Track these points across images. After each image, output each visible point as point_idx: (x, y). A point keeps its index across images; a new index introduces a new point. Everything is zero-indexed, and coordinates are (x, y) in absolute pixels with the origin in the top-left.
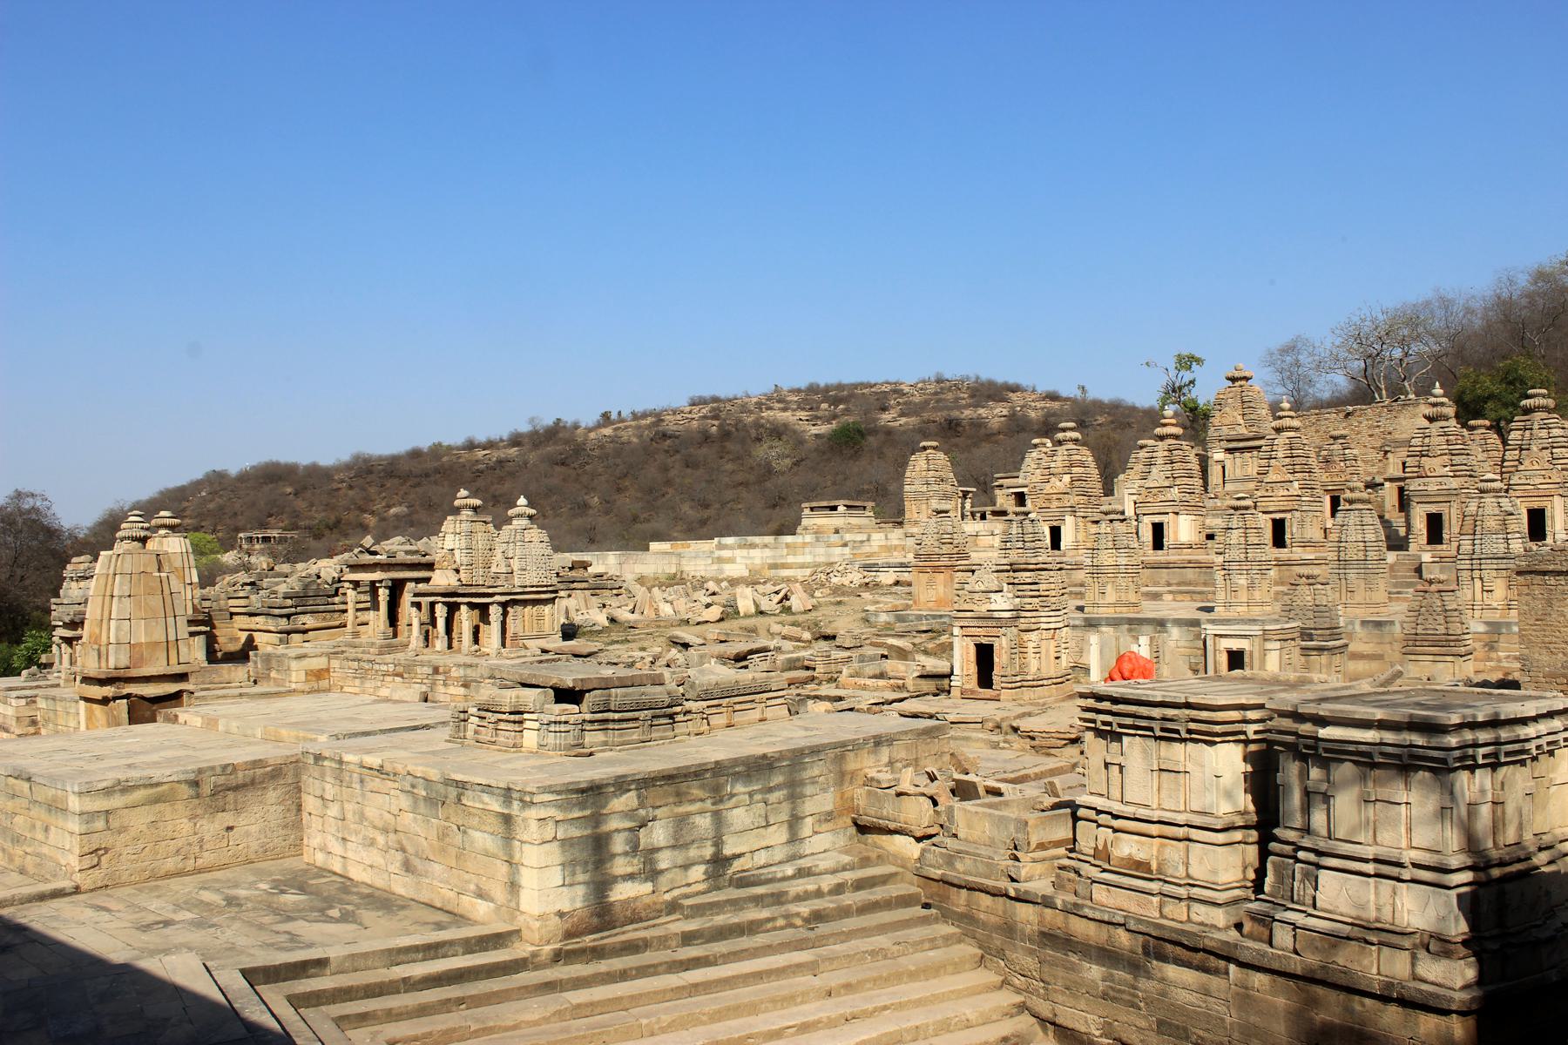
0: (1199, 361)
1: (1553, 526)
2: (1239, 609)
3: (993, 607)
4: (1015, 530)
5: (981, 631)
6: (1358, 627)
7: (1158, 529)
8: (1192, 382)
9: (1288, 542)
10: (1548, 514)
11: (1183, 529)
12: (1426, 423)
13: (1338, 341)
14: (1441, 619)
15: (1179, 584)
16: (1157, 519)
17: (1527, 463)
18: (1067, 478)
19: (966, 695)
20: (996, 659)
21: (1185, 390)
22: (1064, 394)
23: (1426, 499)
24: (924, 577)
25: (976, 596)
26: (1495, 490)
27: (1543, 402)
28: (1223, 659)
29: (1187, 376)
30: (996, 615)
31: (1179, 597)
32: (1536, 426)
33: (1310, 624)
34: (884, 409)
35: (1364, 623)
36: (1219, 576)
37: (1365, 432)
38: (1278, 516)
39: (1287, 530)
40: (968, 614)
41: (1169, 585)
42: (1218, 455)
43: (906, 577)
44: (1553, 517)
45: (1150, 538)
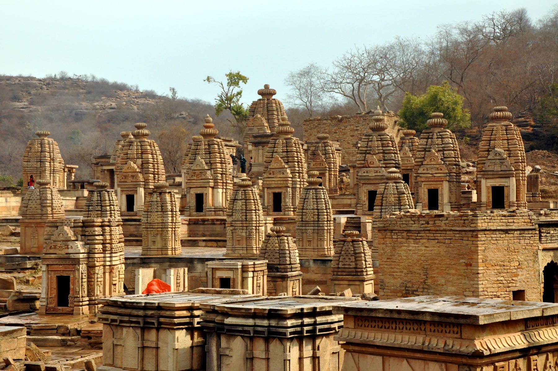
0: (245, 80)
1: (442, 200)
2: (241, 252)
3: (70, 251)
4: (95, 197)
5: (61, 268)
6: (311, 263)
7: (200, 198)
8: (239, 93)
9: (283, 208)
10: (440, 193)
11: (218, 198)
12: (371, 132)
13: (337, 70)
14: (353, 258)
15: (210, 235)
16: (199, 191)
17: (428, 160)
18: (139, 161)
19: (49, 312)
20: (71, 286)
21: (235, 99)
22: (159, 93)
23: (367, 181)
24: (29, 231)
25: (59, 244)
26: (395, 178)
27: (440, 120)
28: (217, 283)
29: (236, 90)
30: (72, 256)
31: (210, 244)
32: (435, 136)
33: (276, 262)
34: (16, 98)
35: (315, 261)
36: (229, 229)
37: (349, 133)
38: (277, 191)
39: (283, 200)
40: (53, 256)
41: (204, 236)
42: (250, 147)
43: (18, 230)
44: (442, 195)
45: (195, 204)
